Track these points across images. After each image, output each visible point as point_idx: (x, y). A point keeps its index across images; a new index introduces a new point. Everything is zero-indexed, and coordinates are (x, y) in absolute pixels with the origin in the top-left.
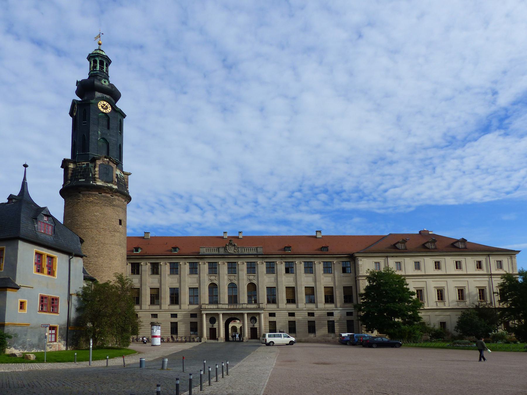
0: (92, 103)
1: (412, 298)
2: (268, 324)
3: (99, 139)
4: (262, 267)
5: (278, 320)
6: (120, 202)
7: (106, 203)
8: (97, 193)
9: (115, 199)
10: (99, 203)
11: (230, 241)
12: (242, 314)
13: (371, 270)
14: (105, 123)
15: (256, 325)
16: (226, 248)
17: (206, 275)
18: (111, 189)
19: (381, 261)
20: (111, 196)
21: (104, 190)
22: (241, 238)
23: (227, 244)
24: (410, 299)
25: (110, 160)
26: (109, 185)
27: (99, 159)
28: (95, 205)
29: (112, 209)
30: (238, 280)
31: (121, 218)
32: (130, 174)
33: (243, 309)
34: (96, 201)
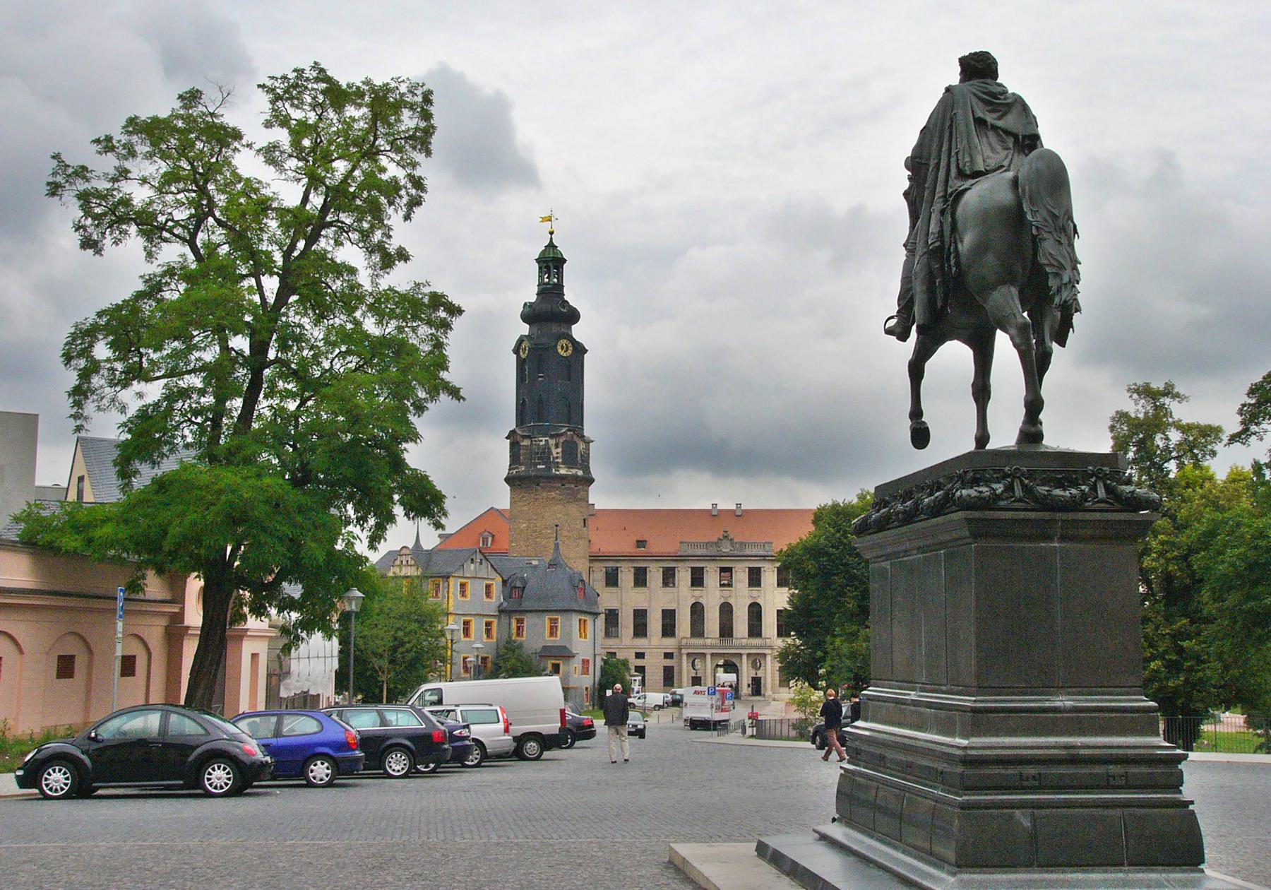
12: (741, 655)
15: (760, 674)
18: (575, 477)
26: (574, 471)
32: (592, 441)
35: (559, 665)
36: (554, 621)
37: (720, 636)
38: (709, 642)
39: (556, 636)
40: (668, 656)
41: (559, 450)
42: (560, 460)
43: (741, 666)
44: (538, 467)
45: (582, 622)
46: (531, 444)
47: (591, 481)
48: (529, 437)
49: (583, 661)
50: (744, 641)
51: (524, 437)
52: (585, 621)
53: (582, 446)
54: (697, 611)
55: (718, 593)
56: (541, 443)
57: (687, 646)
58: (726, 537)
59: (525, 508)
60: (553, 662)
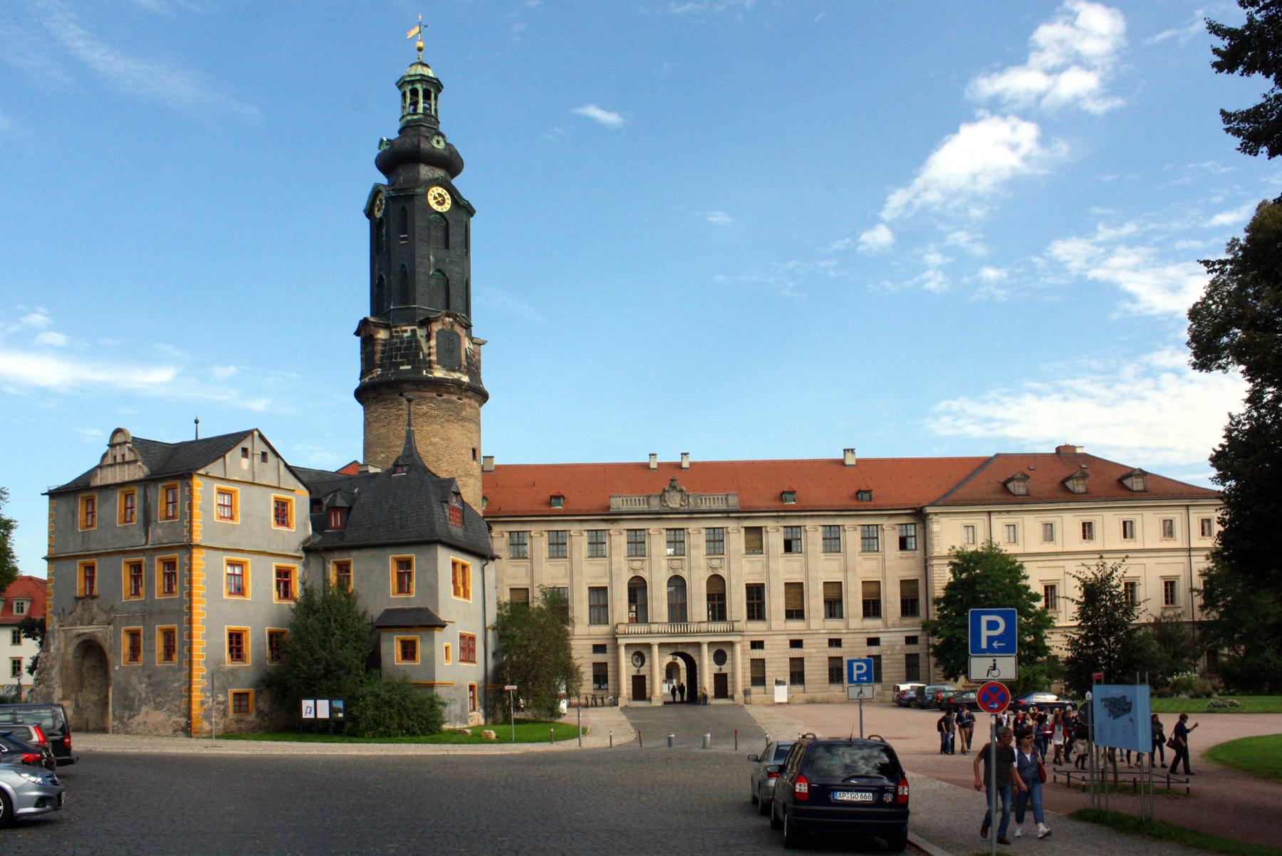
0: (418, 195)
1: (1033, 607)
2: (749, 665)
3: (431, 273)
4: (736, 539)
5: (770, 656)
6: (472, 410)
7: (450, 415)
8: (435, 395)
9: (464, 404)
10: (438, 415)
11: (672, 480)
13: (958, 548)
14: (440, 234)
16: (664, 496)
17: (623, 559)
18: (458, 383)
19: (979, 522)
20: (459, 399)
21: (448, 388)
22: (687, 469)
23: (667, 488)
24: (1030, 609)
25: (455, 319)
26: (456, 375)
27: (436, 320)
28: (432, 422)
29: (460, 428)
30: (690, 569)
31: (474, 446)
33: (699, 633)
34: (433, 412)
35: (413, 643)
36: (405, 564)
37: (669, 622)
38: (655, 628)
39: (409, 592)
40: (599, 649)
41: (433, 343)
42: (434, 358)
43: (701, 660)
44: (401, 368)
45: (459, 568)
46: (392, 337)
47: (483, 396)
48: (387, 327)
49: (462, 637)
50: (704, 627)
51: (377, 326)
52: (464, 567)
53: (466, 344)
54: (637, 589)
55: (664, 563)
56: (406, 335)
57: (626, 635)
58: (674, 488)
59: (383, 430)
60: (403, 637)
